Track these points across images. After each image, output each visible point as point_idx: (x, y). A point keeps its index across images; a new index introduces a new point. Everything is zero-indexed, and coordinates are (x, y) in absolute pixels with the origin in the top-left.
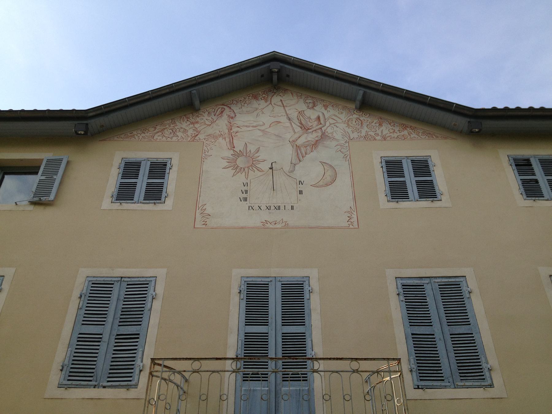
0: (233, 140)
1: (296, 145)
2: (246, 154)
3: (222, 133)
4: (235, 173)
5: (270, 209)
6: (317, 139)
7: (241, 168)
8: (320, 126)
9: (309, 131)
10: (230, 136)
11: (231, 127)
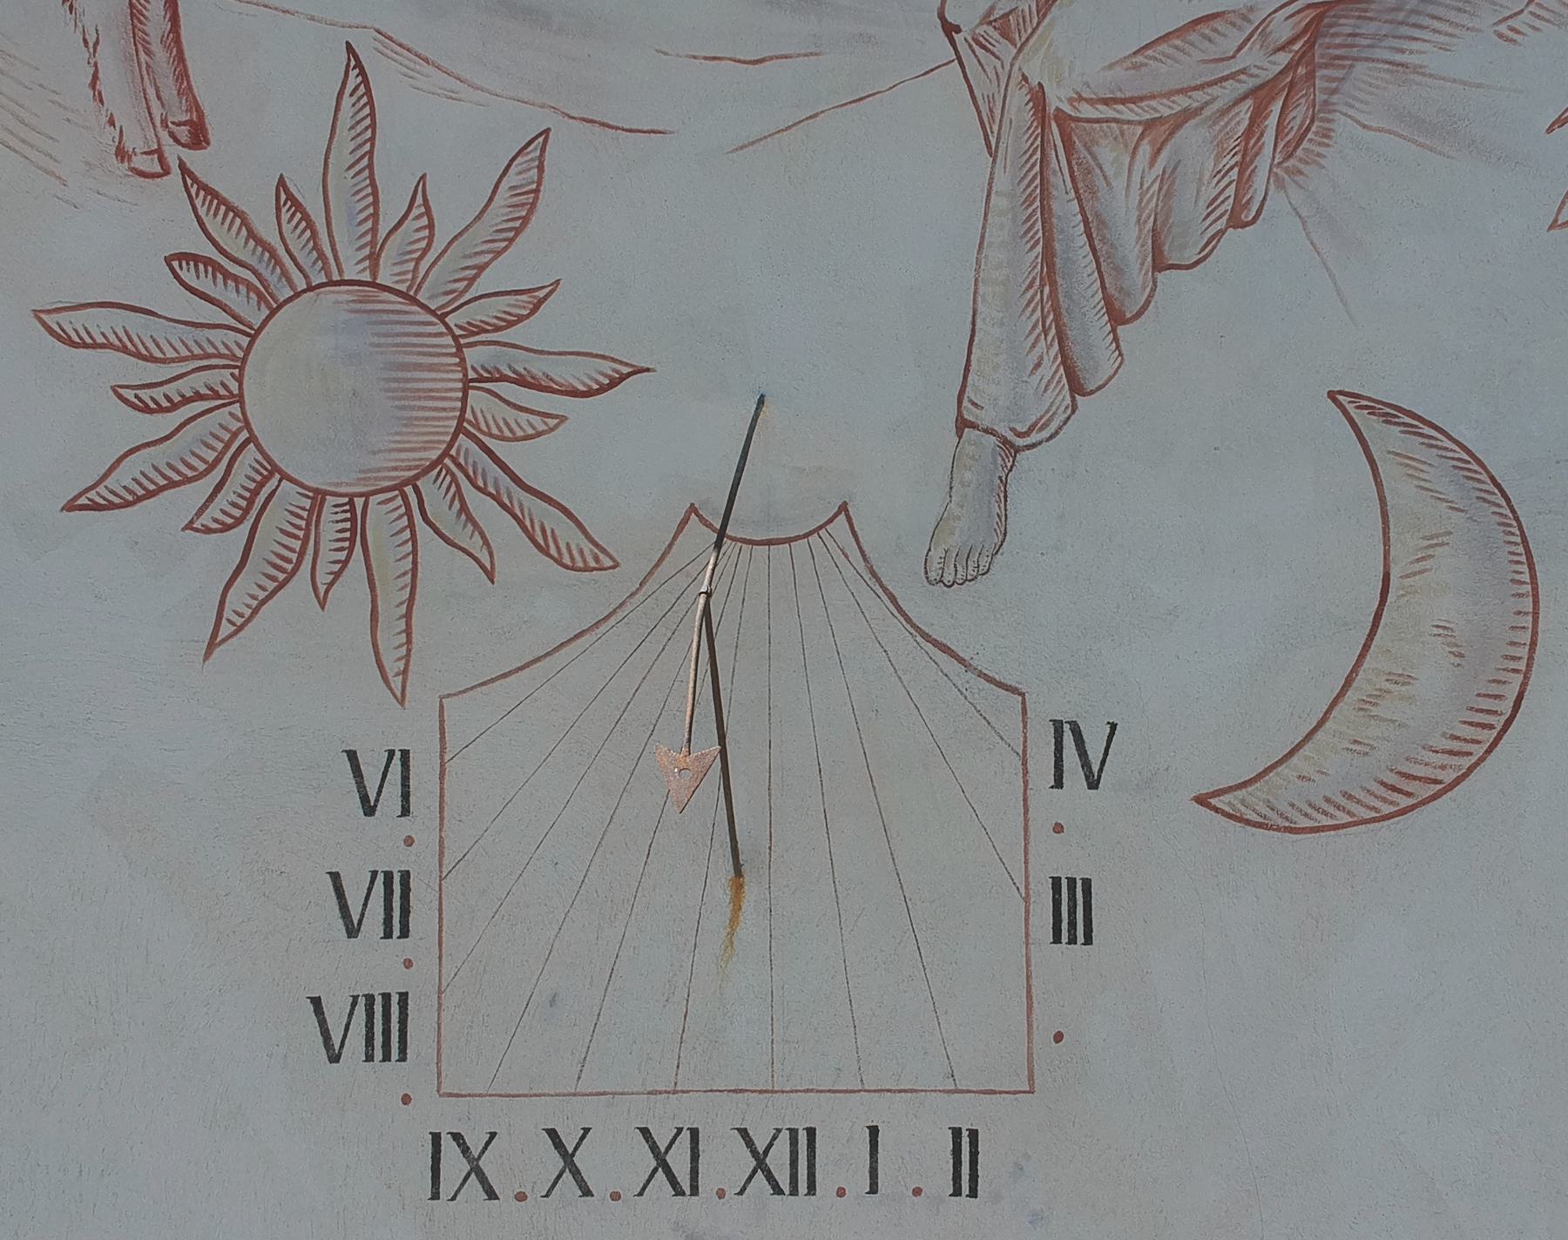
1: (1038, 98)
2: (374, 259)
4: (238, 600)
7: (319, 496)
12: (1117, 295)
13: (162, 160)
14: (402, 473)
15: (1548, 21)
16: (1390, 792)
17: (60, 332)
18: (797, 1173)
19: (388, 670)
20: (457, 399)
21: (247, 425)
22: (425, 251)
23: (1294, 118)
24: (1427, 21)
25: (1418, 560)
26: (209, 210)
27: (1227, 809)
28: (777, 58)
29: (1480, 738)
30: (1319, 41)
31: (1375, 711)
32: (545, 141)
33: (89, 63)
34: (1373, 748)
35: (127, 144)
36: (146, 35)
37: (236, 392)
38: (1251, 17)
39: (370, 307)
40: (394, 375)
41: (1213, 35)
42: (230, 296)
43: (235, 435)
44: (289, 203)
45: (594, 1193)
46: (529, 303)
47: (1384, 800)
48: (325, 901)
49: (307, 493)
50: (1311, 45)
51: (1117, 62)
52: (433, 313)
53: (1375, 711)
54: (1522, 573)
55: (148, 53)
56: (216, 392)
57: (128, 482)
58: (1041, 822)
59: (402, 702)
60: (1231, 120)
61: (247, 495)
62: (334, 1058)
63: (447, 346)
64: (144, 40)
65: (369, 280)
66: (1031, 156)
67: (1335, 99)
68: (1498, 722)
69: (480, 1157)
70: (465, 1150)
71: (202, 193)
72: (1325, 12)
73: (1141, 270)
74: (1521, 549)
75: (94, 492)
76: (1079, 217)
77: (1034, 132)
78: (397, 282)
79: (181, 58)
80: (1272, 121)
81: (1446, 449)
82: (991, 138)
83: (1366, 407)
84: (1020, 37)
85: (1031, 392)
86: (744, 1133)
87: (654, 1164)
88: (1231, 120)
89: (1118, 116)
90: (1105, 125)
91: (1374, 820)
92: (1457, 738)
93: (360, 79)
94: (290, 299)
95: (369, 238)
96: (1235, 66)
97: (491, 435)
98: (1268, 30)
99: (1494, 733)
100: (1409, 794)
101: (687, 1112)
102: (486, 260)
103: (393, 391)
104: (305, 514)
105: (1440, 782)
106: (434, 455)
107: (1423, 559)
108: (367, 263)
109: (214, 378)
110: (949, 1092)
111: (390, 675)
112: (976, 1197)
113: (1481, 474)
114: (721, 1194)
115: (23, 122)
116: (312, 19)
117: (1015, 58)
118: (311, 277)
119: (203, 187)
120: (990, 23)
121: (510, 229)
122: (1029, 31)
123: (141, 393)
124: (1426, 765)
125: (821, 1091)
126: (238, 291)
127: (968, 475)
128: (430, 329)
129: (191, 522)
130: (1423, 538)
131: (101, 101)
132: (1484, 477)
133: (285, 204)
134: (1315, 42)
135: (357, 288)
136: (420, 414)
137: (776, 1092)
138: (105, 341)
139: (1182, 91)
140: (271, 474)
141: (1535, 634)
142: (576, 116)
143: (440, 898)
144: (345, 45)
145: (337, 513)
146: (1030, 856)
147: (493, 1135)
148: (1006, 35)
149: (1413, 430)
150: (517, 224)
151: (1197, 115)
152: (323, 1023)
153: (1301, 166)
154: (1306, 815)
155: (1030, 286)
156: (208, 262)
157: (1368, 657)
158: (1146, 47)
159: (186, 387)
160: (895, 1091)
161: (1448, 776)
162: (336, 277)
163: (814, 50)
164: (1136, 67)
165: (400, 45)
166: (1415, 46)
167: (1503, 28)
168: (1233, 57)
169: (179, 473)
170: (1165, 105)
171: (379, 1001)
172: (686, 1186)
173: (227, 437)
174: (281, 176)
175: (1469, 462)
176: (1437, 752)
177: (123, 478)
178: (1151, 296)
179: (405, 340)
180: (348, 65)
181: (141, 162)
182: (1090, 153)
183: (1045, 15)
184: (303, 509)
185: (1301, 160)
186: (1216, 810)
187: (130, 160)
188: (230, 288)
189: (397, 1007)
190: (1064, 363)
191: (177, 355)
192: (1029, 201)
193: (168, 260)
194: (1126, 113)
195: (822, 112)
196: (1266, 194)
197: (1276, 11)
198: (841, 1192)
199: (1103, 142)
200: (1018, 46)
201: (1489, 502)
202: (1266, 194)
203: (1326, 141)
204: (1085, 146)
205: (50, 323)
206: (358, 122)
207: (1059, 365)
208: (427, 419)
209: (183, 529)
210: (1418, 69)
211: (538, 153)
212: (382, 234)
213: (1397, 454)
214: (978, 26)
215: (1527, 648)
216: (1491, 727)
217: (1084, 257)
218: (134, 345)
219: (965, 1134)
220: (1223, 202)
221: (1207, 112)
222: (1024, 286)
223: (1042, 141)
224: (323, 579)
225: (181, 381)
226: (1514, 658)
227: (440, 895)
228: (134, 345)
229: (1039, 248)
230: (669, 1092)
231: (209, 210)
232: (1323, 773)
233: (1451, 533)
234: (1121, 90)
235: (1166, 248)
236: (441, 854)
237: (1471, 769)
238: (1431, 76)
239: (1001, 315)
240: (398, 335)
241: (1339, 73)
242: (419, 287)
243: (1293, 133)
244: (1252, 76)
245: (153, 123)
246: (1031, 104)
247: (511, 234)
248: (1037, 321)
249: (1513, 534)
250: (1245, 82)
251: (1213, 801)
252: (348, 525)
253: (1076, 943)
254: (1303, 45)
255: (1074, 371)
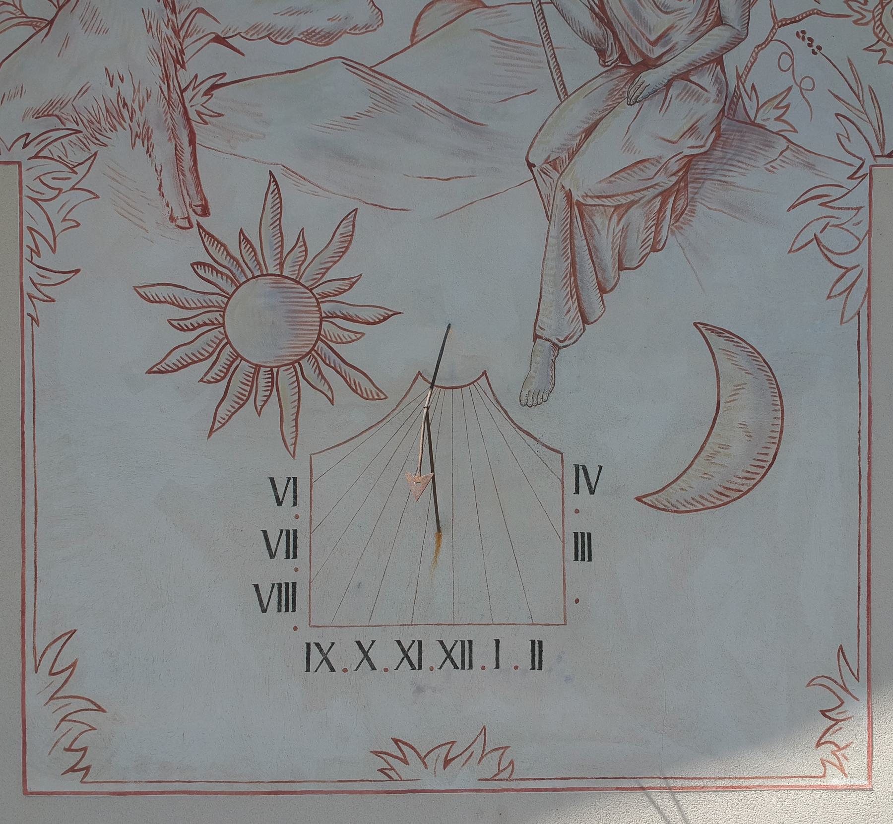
0: (194, 154)
1: (569, 195)
2: (281, 265)
3: (127, 93)
4: (223, 412)
5: (420, 660)
6: (690, 144)
7: (257, 368)
8: (719, 36)
9: (652, 78)
10: (178, 116)
11: (175, 41)
12: (603, 281)
13: (189, 221)
14: (293, 358)
15: (787, 163)
16: (720, 495)
17: (145, 296)
18: (464, 660)
19: (287, 443)
20: (317, 326)
21: (227, 337)
22: (304, 261)
23: (679, 204)
24: (735, 163)
25: (732, 395)
26: (210, 243)
27: (650, 503)
28: (456, 178)
29: (758, 472)
30: (690, 171)
31: (713, 460)
32: (356, 214)
33: (158, 179)
34: (712, 476)
35: (174, 215)
36: (183, 167)
37: (222, 322)
38: (661, 161)
39: (280, 285)
40: (290, 315)
41: (644, 169)
42: (219, 280)
43: (221, 341)
44: (245, 240)
45: (377, 668)
46: (349, 284)
47: (717, 499)
48: (260, 542)
49: (252, 366)
50: (686, 173)
51: (603, 180)
52: (307, 288)
53: (713, 460)
54: (776, 401)
55: (184, 175)
56: (213, 322)
57: (175, 361)
58: (570, 510)
59: (294, 456)
60: (652, 205)
61: (226, 367)
62: (264, 611)
63: (313, 303)
64: (182, 170)
65: (279, 274)
66: (566, 221)
67: (696, 196)
68: (767, 465)
69: (327, 653)
70: (321, 650)
71: (207, 236)
72: (692, 159)
73: (613, 270)
74: (776, 391)
75: (160, 365)
76: (587, 247)
77: (567, 210)
78: (291, 275)
79: (198, 177)
80: (670, 206)
81: (744, 347)
82: (548, 213)
83: (710, 329)
84: (561, 169)
85: (566, 323)
86: (441, 642)
87: (403, 656)
88: (652, 205)
89: (603, 203)
90: (598, 207)
91: (713, 507)
92: (749, 472)
93: (275, 187)
94: (245, 282)
95: (279, 255)
96: (654, 182)
97: (332, 341)
98: (668, 166)
99: (765, 470)
100: (728, 496)
101: (417, 633)
102: (330, 265)
103: (290, 322)
104: (252, 375)
105: (741, 491)
106: (308, 350)
107: (735, 395)
108: (278, 267)
109: (212, 316)
110: (529, 625)
111: (288, 445)
112: (542, 670)
113: (759, 358)
114: (432, 669)
115: (129, 205)
116: (255, 160)
117: (559, 178)
118: (254, 272)
119: (207, 233)
120: (548, 163)
121: (340, 252)
122: (565, 167)
123: (180, 322)
124: (735, 483)
125: (475, 625)
126: (222, 279)
127: (538, 358)
128: (305, 295)
129: (202, 378)
130: (734, 386)
131: (163, 196)
132: (760, 359)
133: (243, 241)
134: (688, 171)
135: (274, 277)
136: (301, 332)
137: (456, 625)
138: (165, 300)
139: (631, 193)
140: (237, 358)
141: (782, 427)
142: (369, 203)
143: (310, 541)
144: (269, 172)
145: (265, 375)
146: (565, 523)
147: (333, 644)
148: (555, 168)
149: (730, 339)
150: (343, 250)
151: (637, 203)
152: (259, 596)
153: (682, 225)
154: (684, 505)
155: (565, 277)
156: (209, 266)
157: (710, 438)
158: (616, 173)
159: (200, 320)
160: (506, 624)
161: (745, 489)
162: (265, 272)
163: (472, 175)
164: (610, 182)
165: (293, 172)
166: (731, 174)
167: (768, 166)
168: (653, 178)
169: (197, 357)
170: (624, 199)
171: (284, 586)
172: (416, 665)
173: (218, 341)
174: (241, 228)
175: (754, 353)
176: (740, 478)
177: (173, 359)
178: (617, 281)
179: (295, 300)
180: (270, 181)
181: (181, 223)
182: (592, 220)
183: (571, 160)
184: (251, 373)
185: (682, 223)
186: (645, 503)
187: (175, 221)
188: (219, 277)
189: (292, 588)
190: (580, 310)
191: (196, 306)
192: (565, 240)
193: (192, 265)
194: (607, 202)
195: (475, 201)
196: (667, 238)
197: (671, 159)
198: (483, 668)
199: (597, 215)
200: (560, 173)
201: (763, 370)
202: (667, 238)
203: (693, 215)
204: (589, 216)
205: (141, 292)
206: (275, 206)
207: (578, 311)
208: (304, 334)
209: (199, 382)
210: (732, 184)
211: (352, 219)
212: (285, 254)
213: (723, 350)
214: (542, 164)
215: (779, 433)
216: (763, 467)
217: (589, 264)
218: (177, 302)
219: (537, 643)
220: (648, 241)
221: (642, 202)
222: (563, 277)
223: (571, 214)
224: (259, 403)
225: (197, 318)
226: (773, 438)
227: (310, 540)
228: (177, 302)
229: (569, 261)
230: (409, 625)
231: (210, 243)
232: (691, 487)
233: (746, 384)
234: (604, 192)
235: (624, 260)
236: (311, 523)
237: (755, 485)
238: (737, 187)
239: (553, 289)
240: (291, 298)
241: (699, 185)
242: (301, 277)
243: (679, 211)
244: (661, 186)
245: (186, 206)
246: (566, 198)
247: (341, 254)
248: (569, 292)
249: (773, 384)
250: (657, 189)
251: (644, 499)
252: (270, 380)
253: (584, 561)
254: (683, 173)
255: (584, 314)
